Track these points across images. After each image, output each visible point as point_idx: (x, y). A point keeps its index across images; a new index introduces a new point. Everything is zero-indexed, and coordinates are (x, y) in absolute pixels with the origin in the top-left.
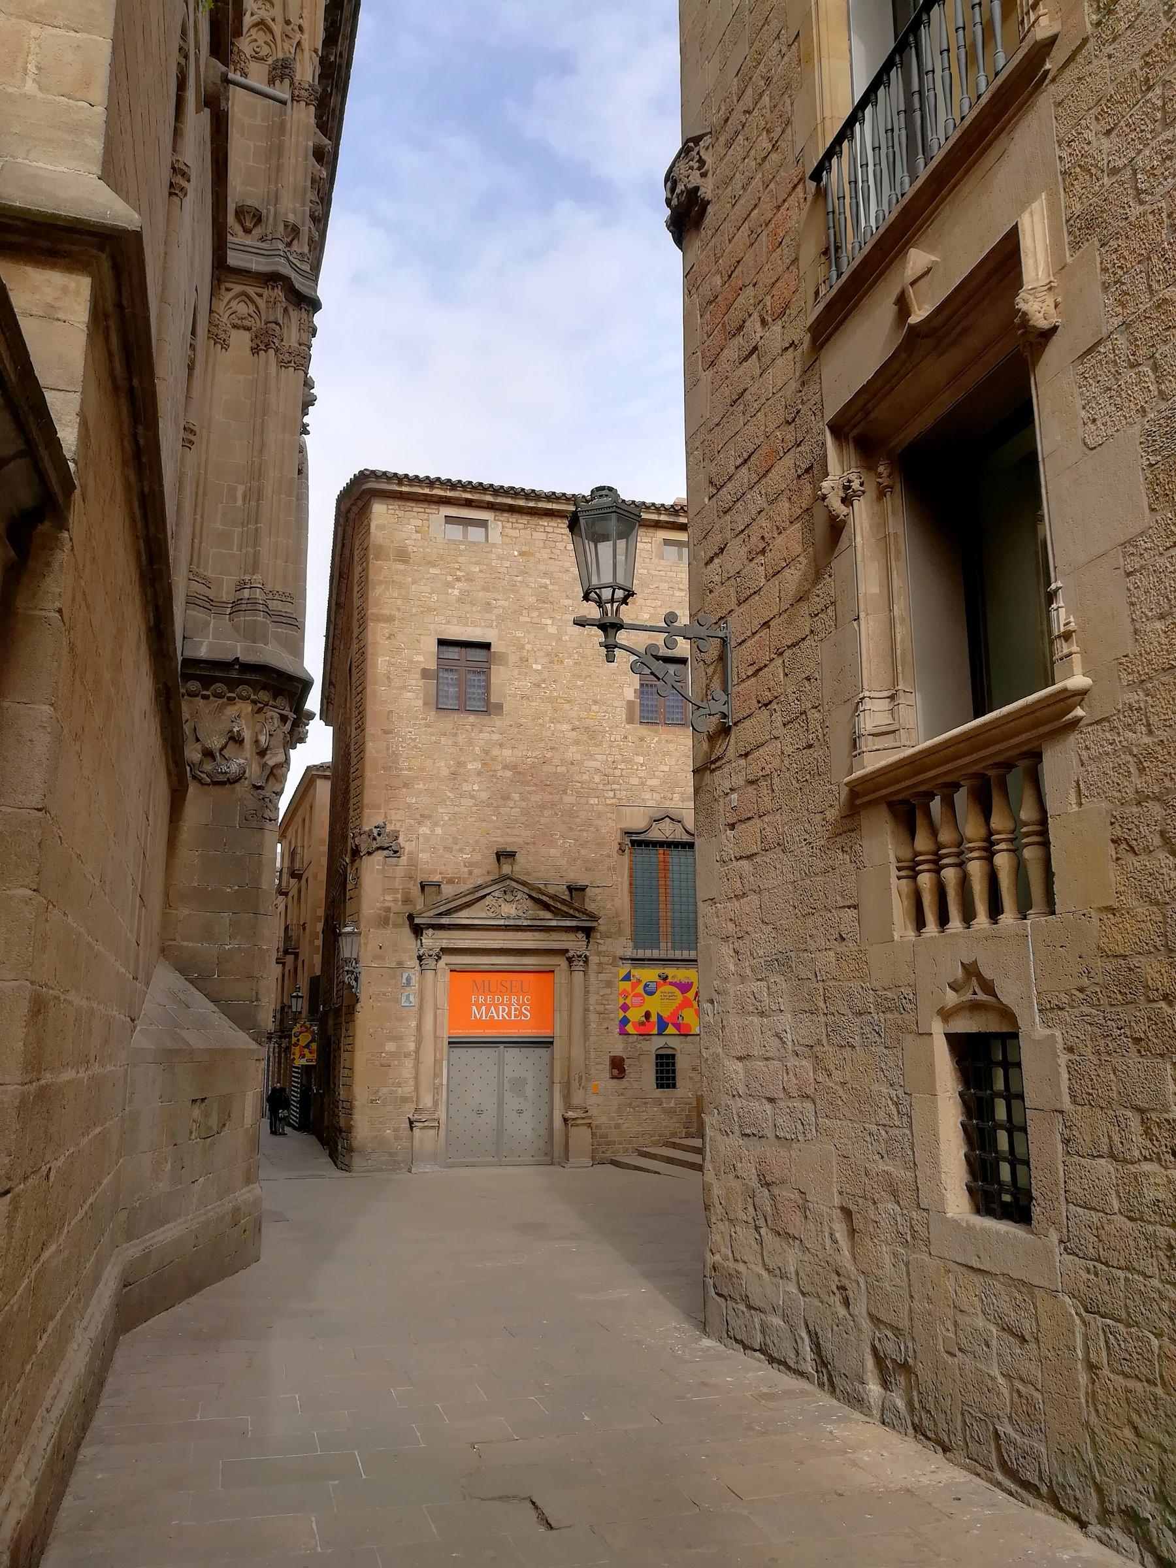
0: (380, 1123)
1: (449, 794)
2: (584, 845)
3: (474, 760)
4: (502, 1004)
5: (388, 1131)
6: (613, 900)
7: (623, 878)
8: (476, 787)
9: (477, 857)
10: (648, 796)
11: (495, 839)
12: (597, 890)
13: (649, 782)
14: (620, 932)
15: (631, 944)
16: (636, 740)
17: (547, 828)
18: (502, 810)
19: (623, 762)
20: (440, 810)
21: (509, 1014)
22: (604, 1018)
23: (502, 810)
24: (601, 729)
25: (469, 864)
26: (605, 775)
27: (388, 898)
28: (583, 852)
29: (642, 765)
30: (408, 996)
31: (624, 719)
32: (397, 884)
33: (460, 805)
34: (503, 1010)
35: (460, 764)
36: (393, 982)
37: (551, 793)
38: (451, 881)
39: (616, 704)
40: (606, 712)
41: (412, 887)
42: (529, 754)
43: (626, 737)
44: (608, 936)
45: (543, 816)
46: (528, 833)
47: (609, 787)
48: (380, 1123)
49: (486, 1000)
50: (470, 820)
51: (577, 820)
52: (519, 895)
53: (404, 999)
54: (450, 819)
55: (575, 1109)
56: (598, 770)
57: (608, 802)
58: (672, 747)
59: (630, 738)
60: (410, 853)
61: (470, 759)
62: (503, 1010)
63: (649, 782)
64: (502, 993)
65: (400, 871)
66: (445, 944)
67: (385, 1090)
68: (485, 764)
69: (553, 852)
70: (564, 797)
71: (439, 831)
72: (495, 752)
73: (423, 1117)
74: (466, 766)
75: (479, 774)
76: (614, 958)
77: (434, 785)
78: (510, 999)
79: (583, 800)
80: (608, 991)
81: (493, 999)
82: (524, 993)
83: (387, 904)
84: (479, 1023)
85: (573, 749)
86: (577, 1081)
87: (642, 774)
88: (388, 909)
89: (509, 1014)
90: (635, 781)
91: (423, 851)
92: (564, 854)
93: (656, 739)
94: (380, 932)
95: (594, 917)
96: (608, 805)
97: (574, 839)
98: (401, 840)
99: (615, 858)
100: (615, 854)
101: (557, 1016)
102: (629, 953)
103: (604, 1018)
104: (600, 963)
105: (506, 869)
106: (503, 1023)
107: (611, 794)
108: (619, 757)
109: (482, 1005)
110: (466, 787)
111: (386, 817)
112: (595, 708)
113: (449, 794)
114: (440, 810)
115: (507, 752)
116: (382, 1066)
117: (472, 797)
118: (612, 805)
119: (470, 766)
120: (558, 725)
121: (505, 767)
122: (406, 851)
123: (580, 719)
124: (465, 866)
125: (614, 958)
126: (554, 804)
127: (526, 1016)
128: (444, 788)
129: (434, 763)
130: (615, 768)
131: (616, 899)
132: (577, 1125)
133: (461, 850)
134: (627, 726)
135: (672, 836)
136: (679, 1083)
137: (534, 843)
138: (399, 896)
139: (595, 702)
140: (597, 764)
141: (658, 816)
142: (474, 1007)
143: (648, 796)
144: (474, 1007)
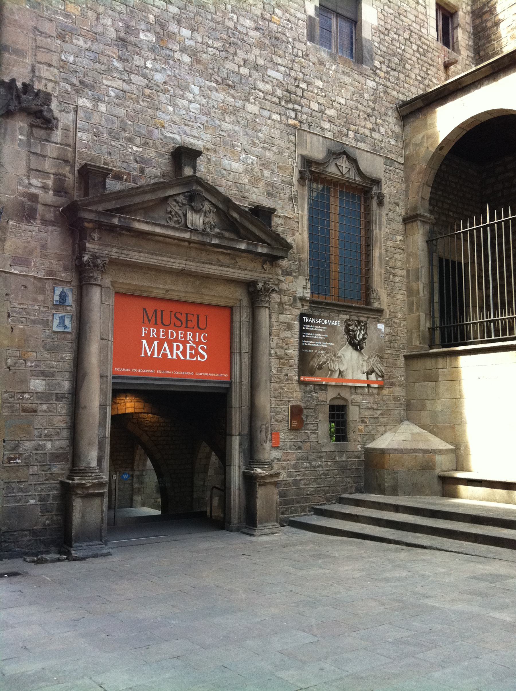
0: (20, 490)
1: (116, 63)
2: (265, 165)
3: (148, 31)
4: (176, 340)
5: (32, 501)
6: (294, 234)
7: (303, 211)
8: (149, 64)
9: (151, 153)
10: (326, 125)
11: (171, 135)
12: (280, 221)
13: (328, 112)
14: (300, 273)
15: (309, 286)
16: (315, 61)
17: (229, 136)
18: (179, 101)
19: (305, 81)
20: (105, 82)
21: (184, 353)
22: (284, 364)
23: (179, 101)
24: (284, 38)
25: (141, 160)
26: (287, 91)
27: (34, 182)
28: (266, 173)
29: (322, 90)
30: (62, 319)
31: (305, 34)
32: (48, 165)
33: (129, 82)
34: (178, 348)
35: (128, 29)
36: (41, 298)
37: (233, 97)
38: (118, 177)
39: (298, 15)
40: (288, 20)
41: (68, 175)
42: (210, 42)
43: (307, 55)
44: (287, 273)
45: (225, 121)
46: (208, 137)
47: (290, 106)
48: (20, 490)
49: (158, 334)
50: (141, 103)
51: (260, 135)
52: (207, 206)
53: (56, 322)
54: (117, 97)
55: (261, 465)
56: (280, 84)
57: (291, 122)
58: (348, 80)
59: (311, 57)
60: (66, 129)
61: (143, 27)
62: (178, 348)
63: (328, 112)
64: (177, 328)
65: (51, 150)
66: (114, 253)
67: (28, 445)
68: (159, 38)
69: (235, 166)
70: (247, 104)
71: (103, 107)
72: (173, 27)
73: (87, 482)
74: (137, 36)
75: (153, 50)
76: (295, 298)
77: (96, 46)
78: (185, 336)
79: (266, 113)
80: (288, 334)
81: (167, 334)
82: (201, 330)
83: (33, 190)
84: (150, 361)
85: (256, 51)
86: (263, 433)
87: (321, 100)
88: (34, 198)
89: (184, 353)
90: (315, 106)
91: (83, 130)
92: (246, 171)
93: (334, 67)
94: (24, 227)
95: (288, 247)
96: (288, 125)
97: (257, 156)
98: (54, 105)
99: (297, 188)
100: (296, 184)
101: (236, 359)
102: (308, 295)
103: (284, 364)
104: (280, 304)
105: (188, 171)
106: (178, 363)
107: (293, 115)
108: (301, 75)
109: (154, 339)
110: (138, 61)
111: (33, 71)
112: (277, 11)
113: (116, 63)
114: (105, 82)
115: (186, 32)
116: (24, 410)
117: (145, 76)
118: (294, 127)
119: (142, 36)
120: (241, 19)
121: (183, 50)
122: (60, 125)
123: (264, 19)
124: (137, 162)
125: (295, 298)
126: (236, 109)
127: (202, 357)
128: (110, 54)
129: (98, 19)
130: (297, 86)
131: (297, 234)
132: (265, 484)
133: (131, 140)
134: (309, 43)
135: (347, 176)
136: (351, 435)
137: (215, 151)
138: (50, 183)
139: (279, 6)
140: (280, 77)
141: (335, 149)
142: (144, 342)
143: (326, 125)
144: (144, 342)
